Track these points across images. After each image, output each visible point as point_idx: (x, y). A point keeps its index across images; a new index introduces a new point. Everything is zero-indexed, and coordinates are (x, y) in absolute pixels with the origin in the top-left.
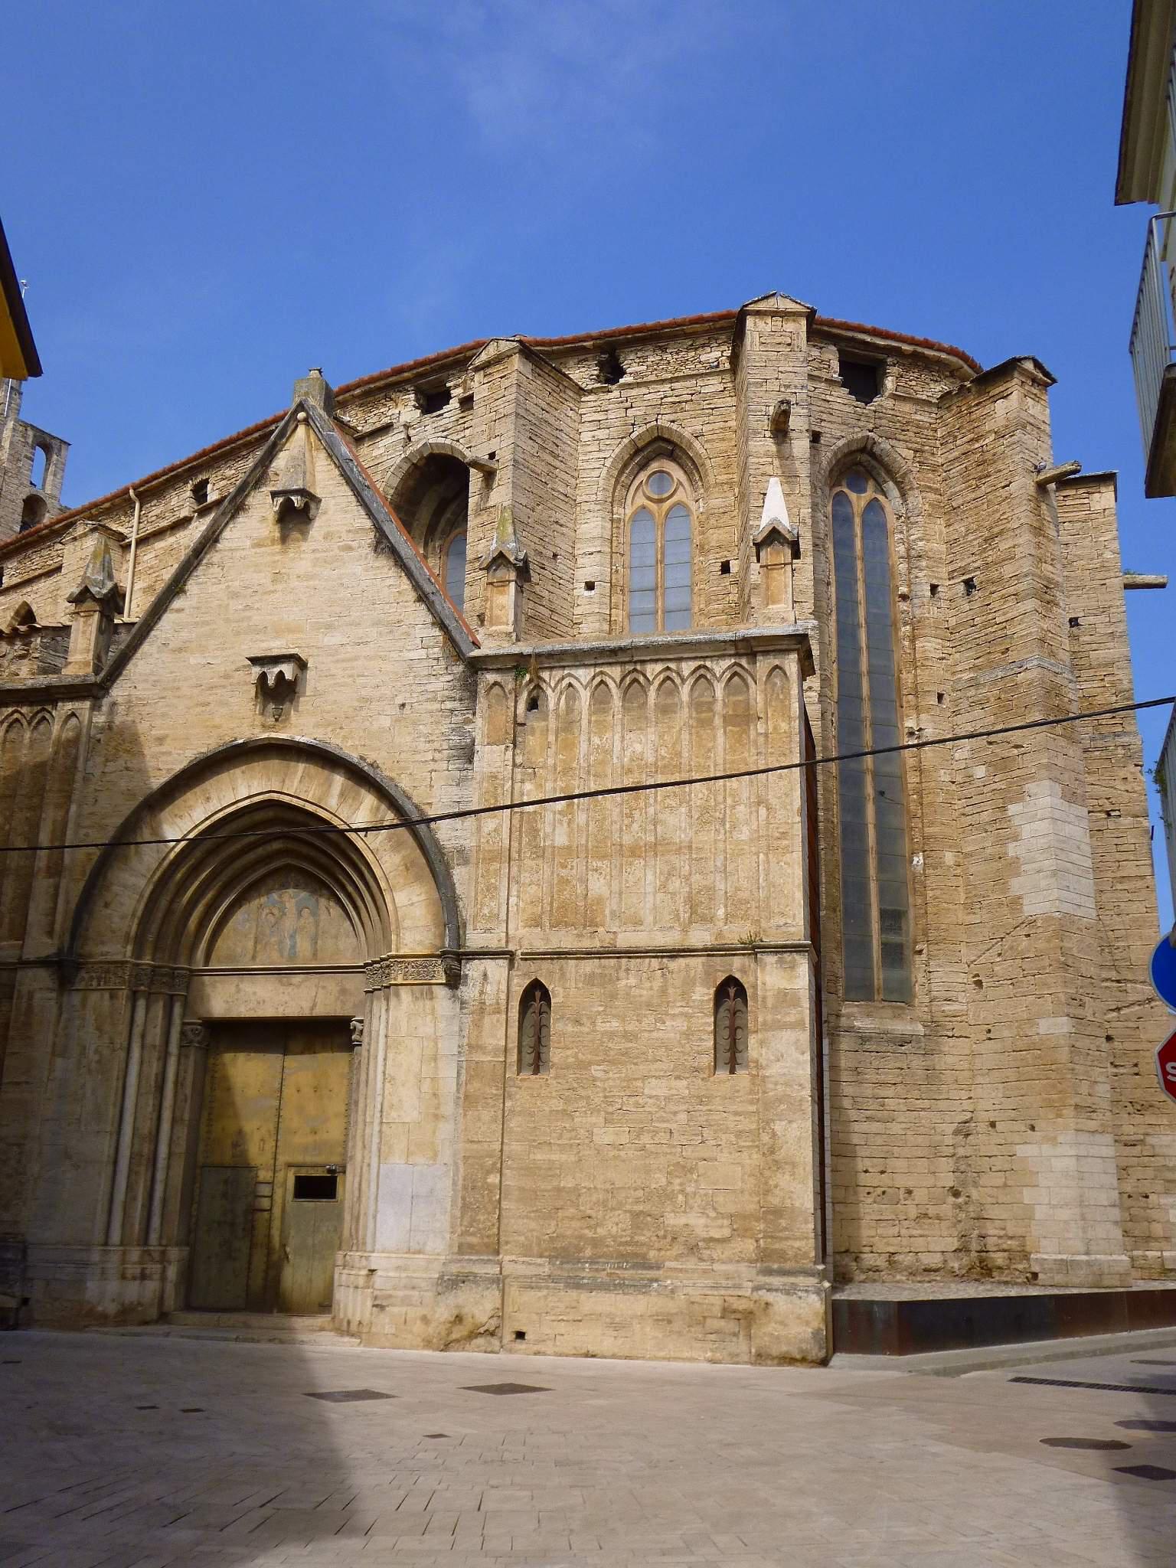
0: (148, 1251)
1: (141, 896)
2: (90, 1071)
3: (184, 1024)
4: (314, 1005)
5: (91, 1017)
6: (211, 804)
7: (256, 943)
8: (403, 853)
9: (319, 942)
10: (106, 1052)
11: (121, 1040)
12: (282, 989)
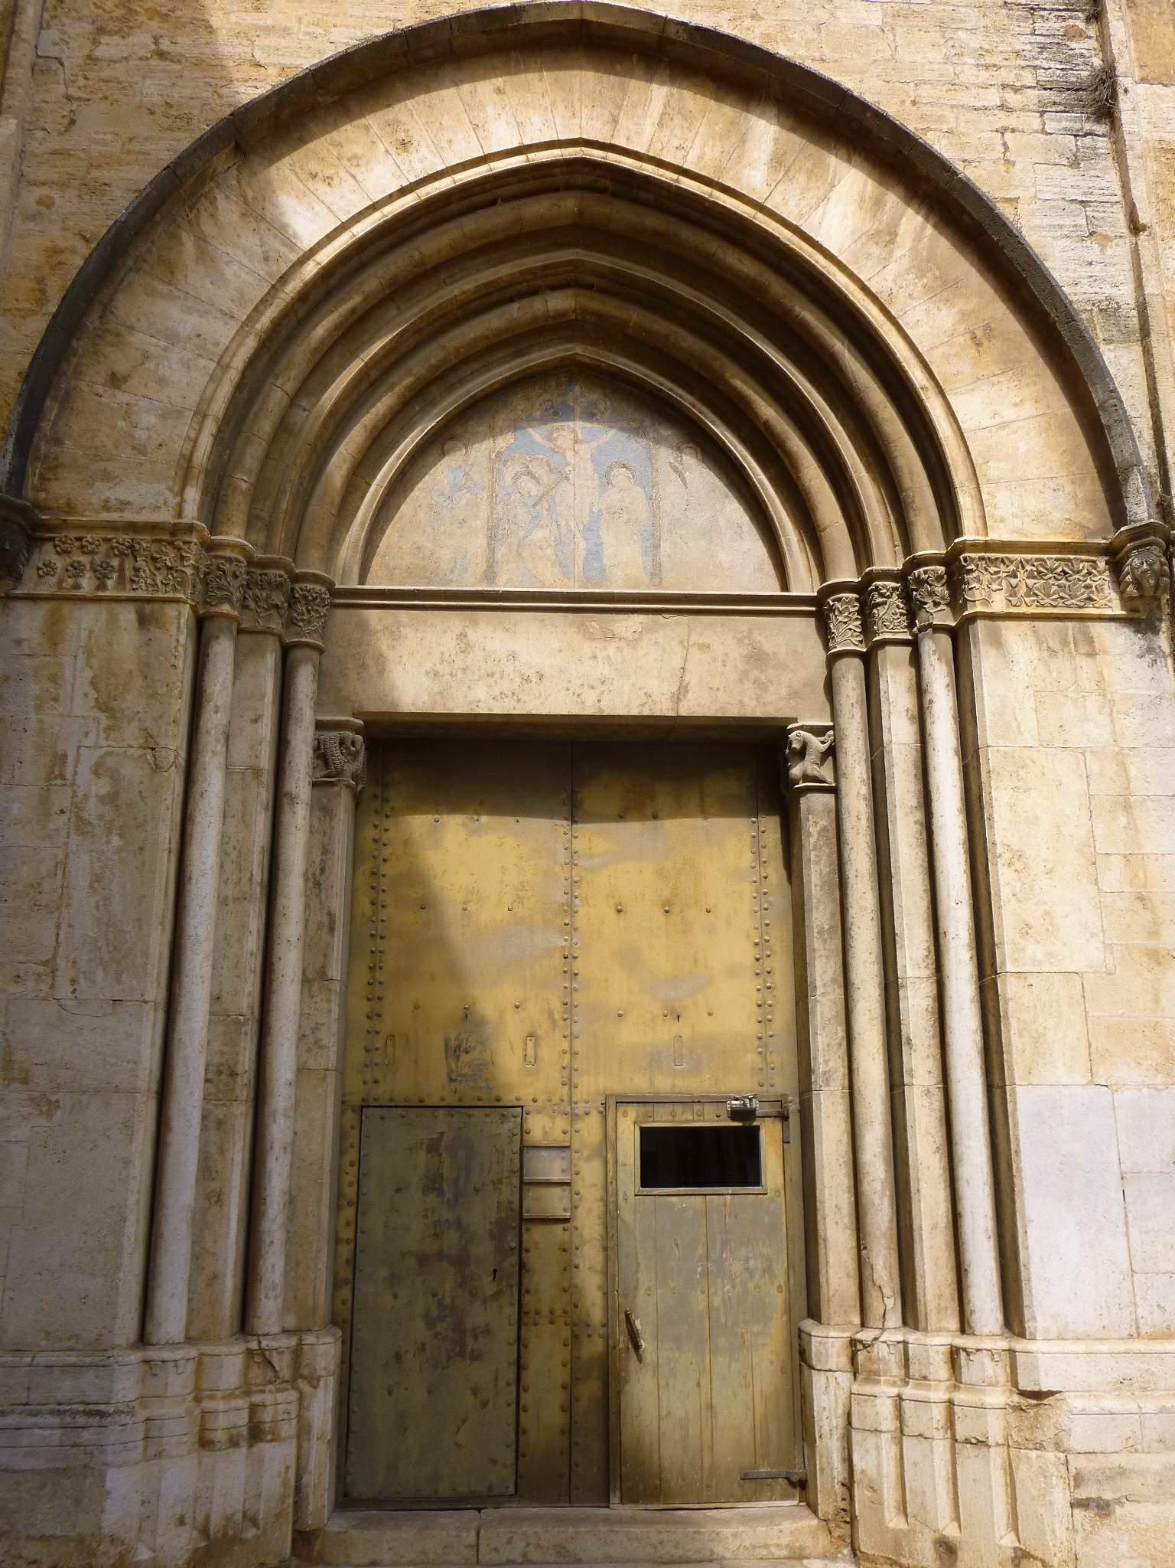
0: (262, 1351)
1: (223, 367)
2: (82, 825)
3: (320, 726)
4: (683, 689)
5: (78, 677)
6: (415, 157)
7: (492, 538)
8: (961, 304)
9: (666, 547)
10: (133, 772)
11: (174, 742)
12: (587, 648)
